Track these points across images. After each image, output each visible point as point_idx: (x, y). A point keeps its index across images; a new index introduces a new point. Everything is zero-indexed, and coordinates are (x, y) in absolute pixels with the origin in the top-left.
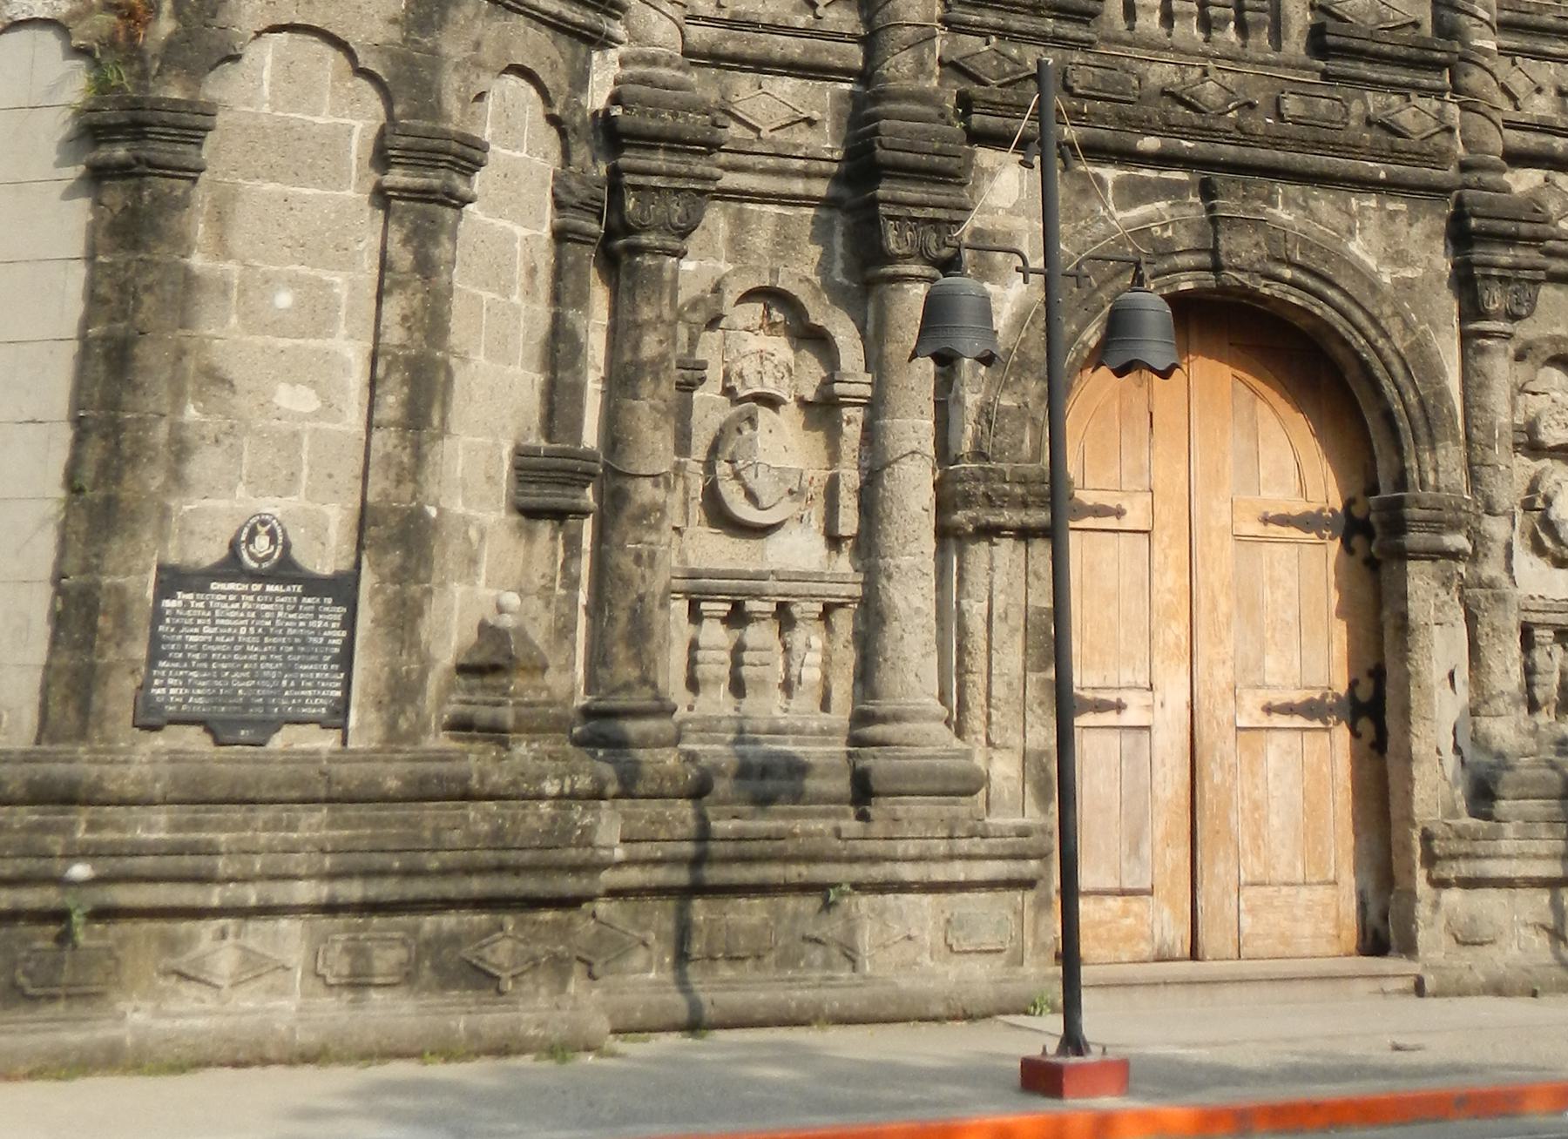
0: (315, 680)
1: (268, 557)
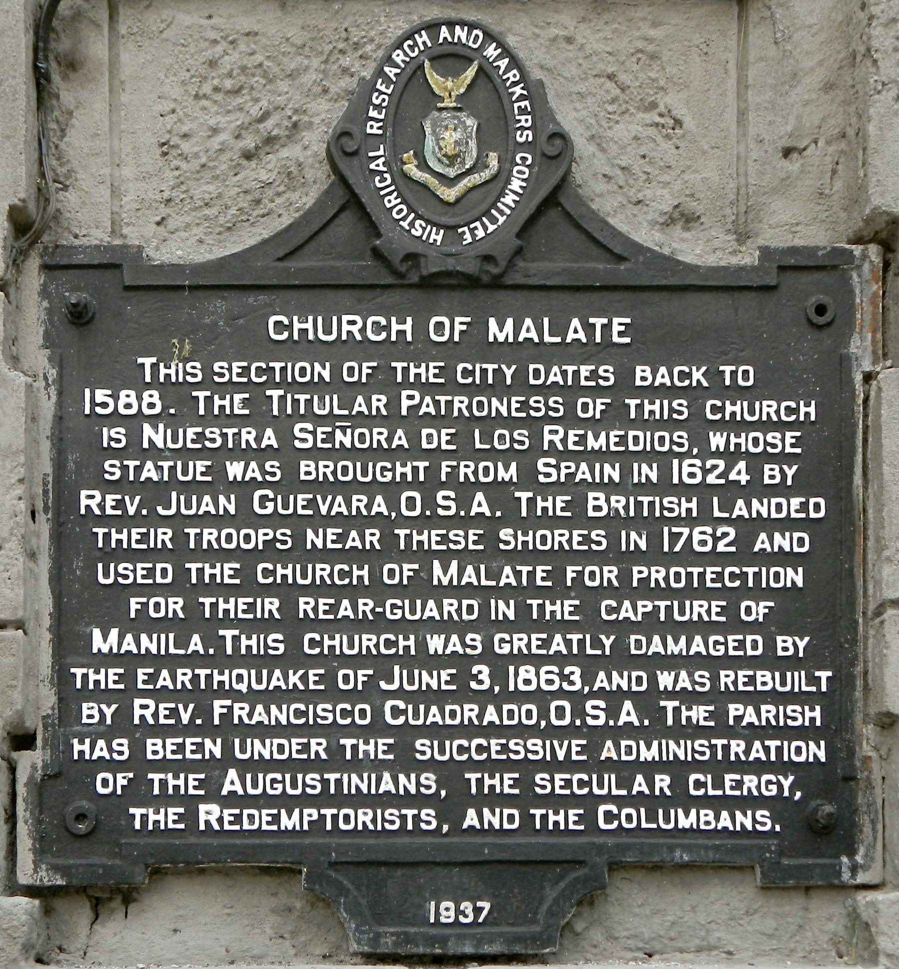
0: (719, 697)
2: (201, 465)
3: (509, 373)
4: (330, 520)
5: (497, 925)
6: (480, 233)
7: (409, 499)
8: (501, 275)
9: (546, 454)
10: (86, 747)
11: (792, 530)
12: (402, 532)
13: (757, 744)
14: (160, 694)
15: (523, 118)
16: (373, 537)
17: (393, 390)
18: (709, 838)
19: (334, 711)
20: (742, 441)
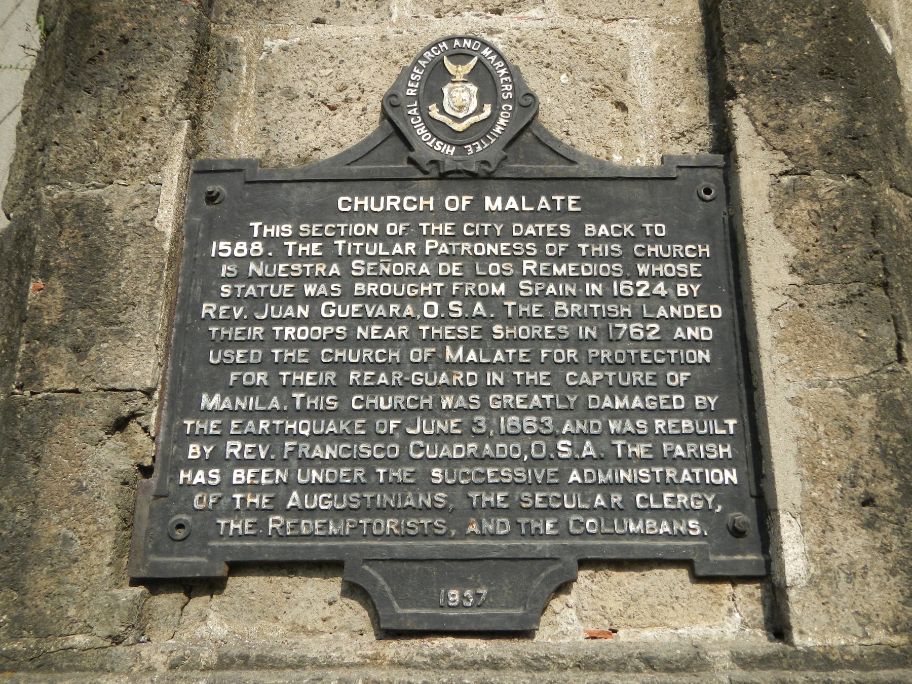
1: (482, 129)
2: (287, 286)
3: (499, 229)
4: (373, 320)
5: (492, 607)
6: (479, 148)
7: (430, 307)
8: (493, 172)
9: (524, 277)
10: (189, 476)
11: (700, 325)
12: (424, 328)
13: (686, 472)
14: (246, 437)
15: (506, 86)
16: (403, 330)
17: (420, 238)
18: (653, 540)
19: (372, 449)
20: (660, 269)
